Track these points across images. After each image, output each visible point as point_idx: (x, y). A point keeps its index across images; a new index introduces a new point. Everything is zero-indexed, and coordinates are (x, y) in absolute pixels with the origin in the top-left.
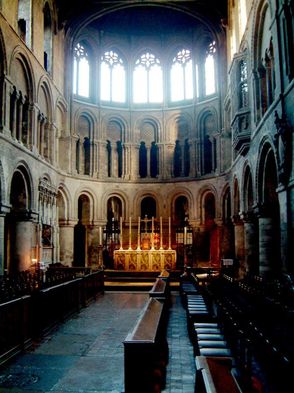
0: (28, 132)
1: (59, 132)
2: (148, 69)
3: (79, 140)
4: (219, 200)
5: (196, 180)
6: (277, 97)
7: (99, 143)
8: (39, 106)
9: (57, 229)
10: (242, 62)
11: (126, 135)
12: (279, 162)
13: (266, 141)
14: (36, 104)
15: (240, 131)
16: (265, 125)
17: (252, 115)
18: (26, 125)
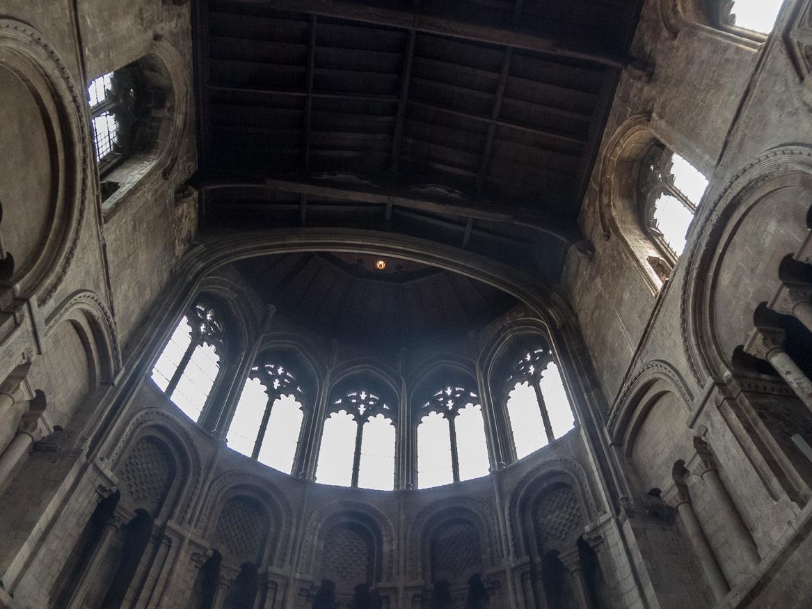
2: (361, 420)
3: (116, 497)
7: (182, 538)
11: (279, 545)
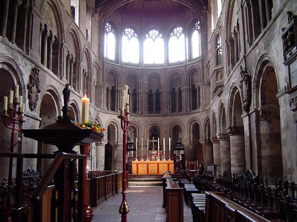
0: (77, 81)
1: (95, 82)
4: (202, 127)
5: (186, 114)
6: (241, 57)
8: (84, 65)
9: (94, 146)
10: (218, 35)
12: (243, 98)
13: (234, 86)
14: (82, 63)
15: (217, 80)
16: (234, 76)
17: (225, 69)
18: (75, 77)
